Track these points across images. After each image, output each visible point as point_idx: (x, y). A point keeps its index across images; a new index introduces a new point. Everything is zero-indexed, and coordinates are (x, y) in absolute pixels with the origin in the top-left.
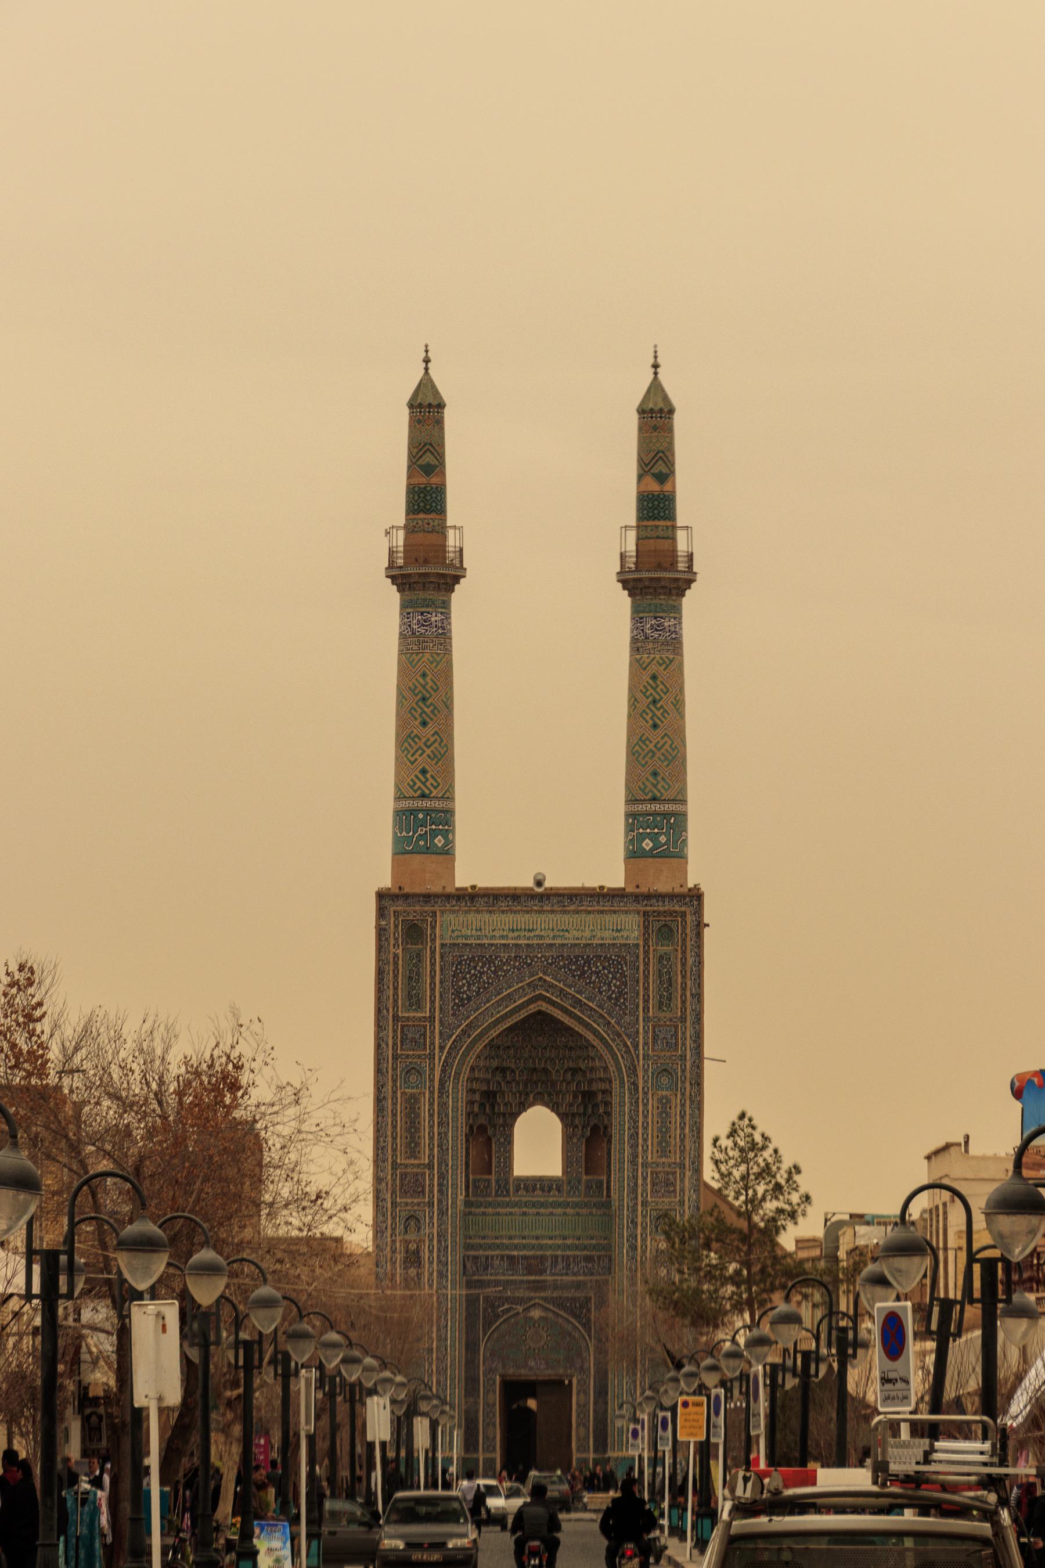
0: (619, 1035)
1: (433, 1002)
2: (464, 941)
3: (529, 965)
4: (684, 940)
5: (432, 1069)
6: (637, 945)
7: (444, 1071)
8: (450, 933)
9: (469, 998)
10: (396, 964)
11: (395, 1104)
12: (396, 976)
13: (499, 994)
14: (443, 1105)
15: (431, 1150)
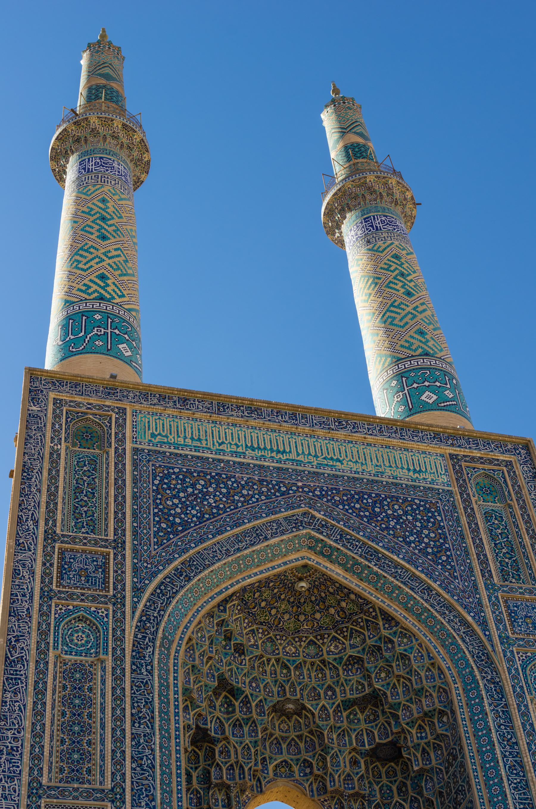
0: (451, 608)
1: (120, 521)
2: (172, 450)
3: (283, 494)
4: (519, 493)
5: (120, 621)
6: (450, 493)
7: (141, 627)
8: (148, 437)
9: (185, 525)
10: (54, 462)
11: (41, 673)
12: (53, 478)
13: (237, 525)
14: (142, 686)
15: (119, 763)
